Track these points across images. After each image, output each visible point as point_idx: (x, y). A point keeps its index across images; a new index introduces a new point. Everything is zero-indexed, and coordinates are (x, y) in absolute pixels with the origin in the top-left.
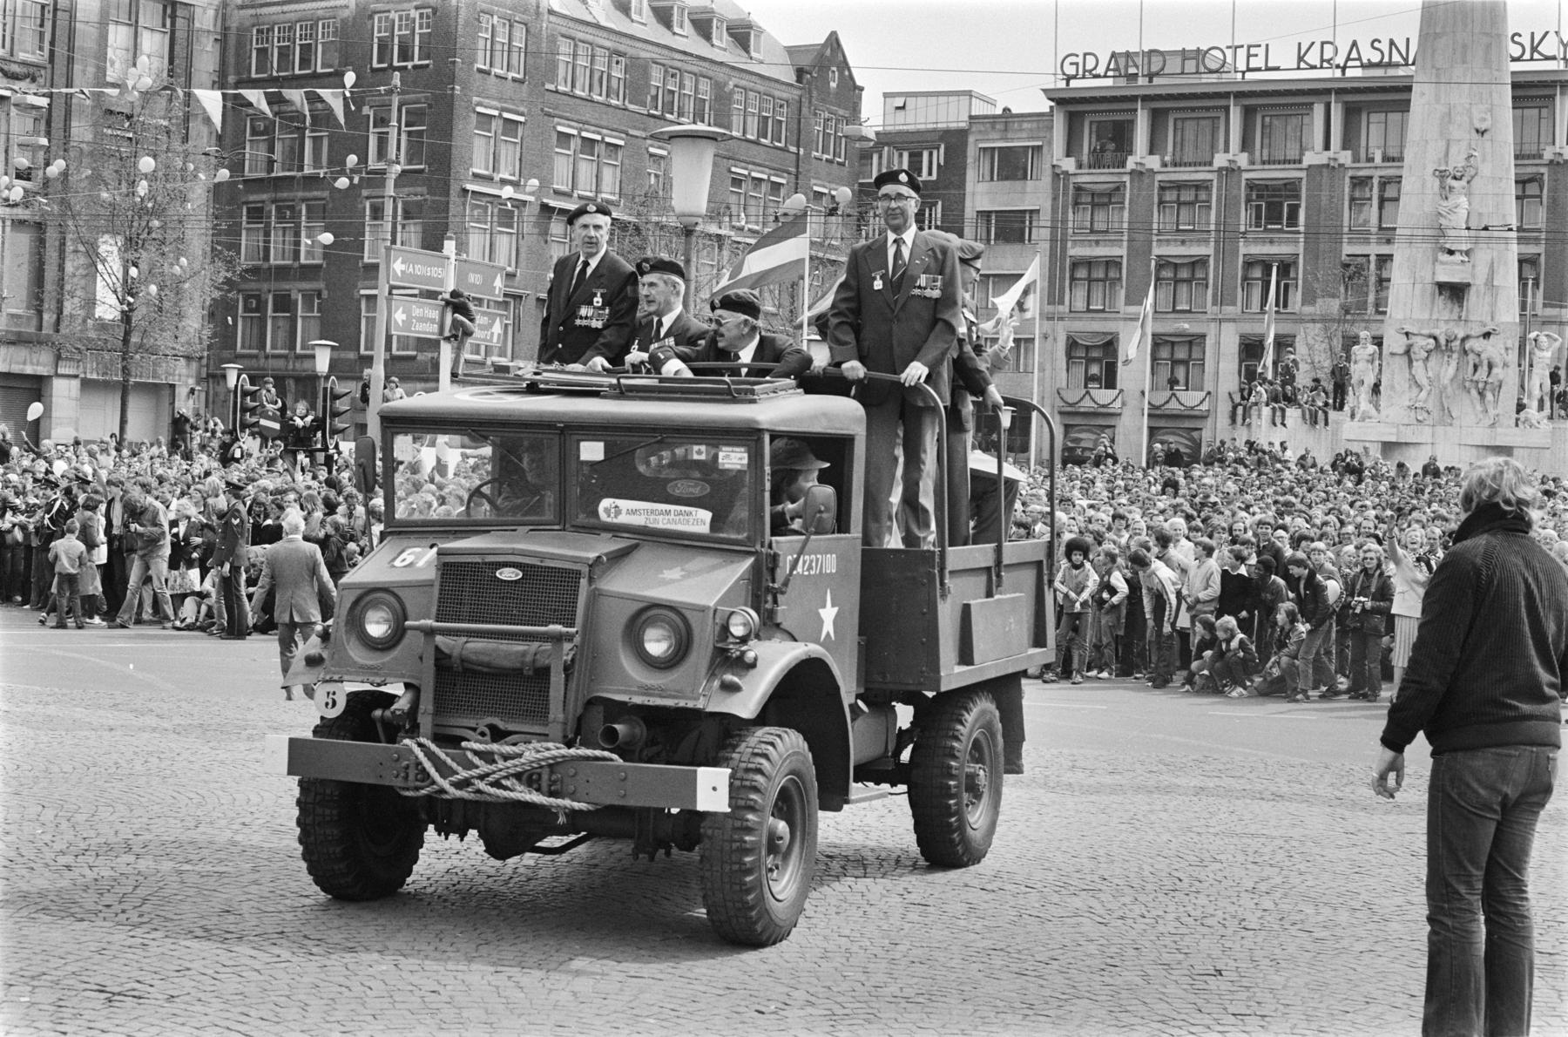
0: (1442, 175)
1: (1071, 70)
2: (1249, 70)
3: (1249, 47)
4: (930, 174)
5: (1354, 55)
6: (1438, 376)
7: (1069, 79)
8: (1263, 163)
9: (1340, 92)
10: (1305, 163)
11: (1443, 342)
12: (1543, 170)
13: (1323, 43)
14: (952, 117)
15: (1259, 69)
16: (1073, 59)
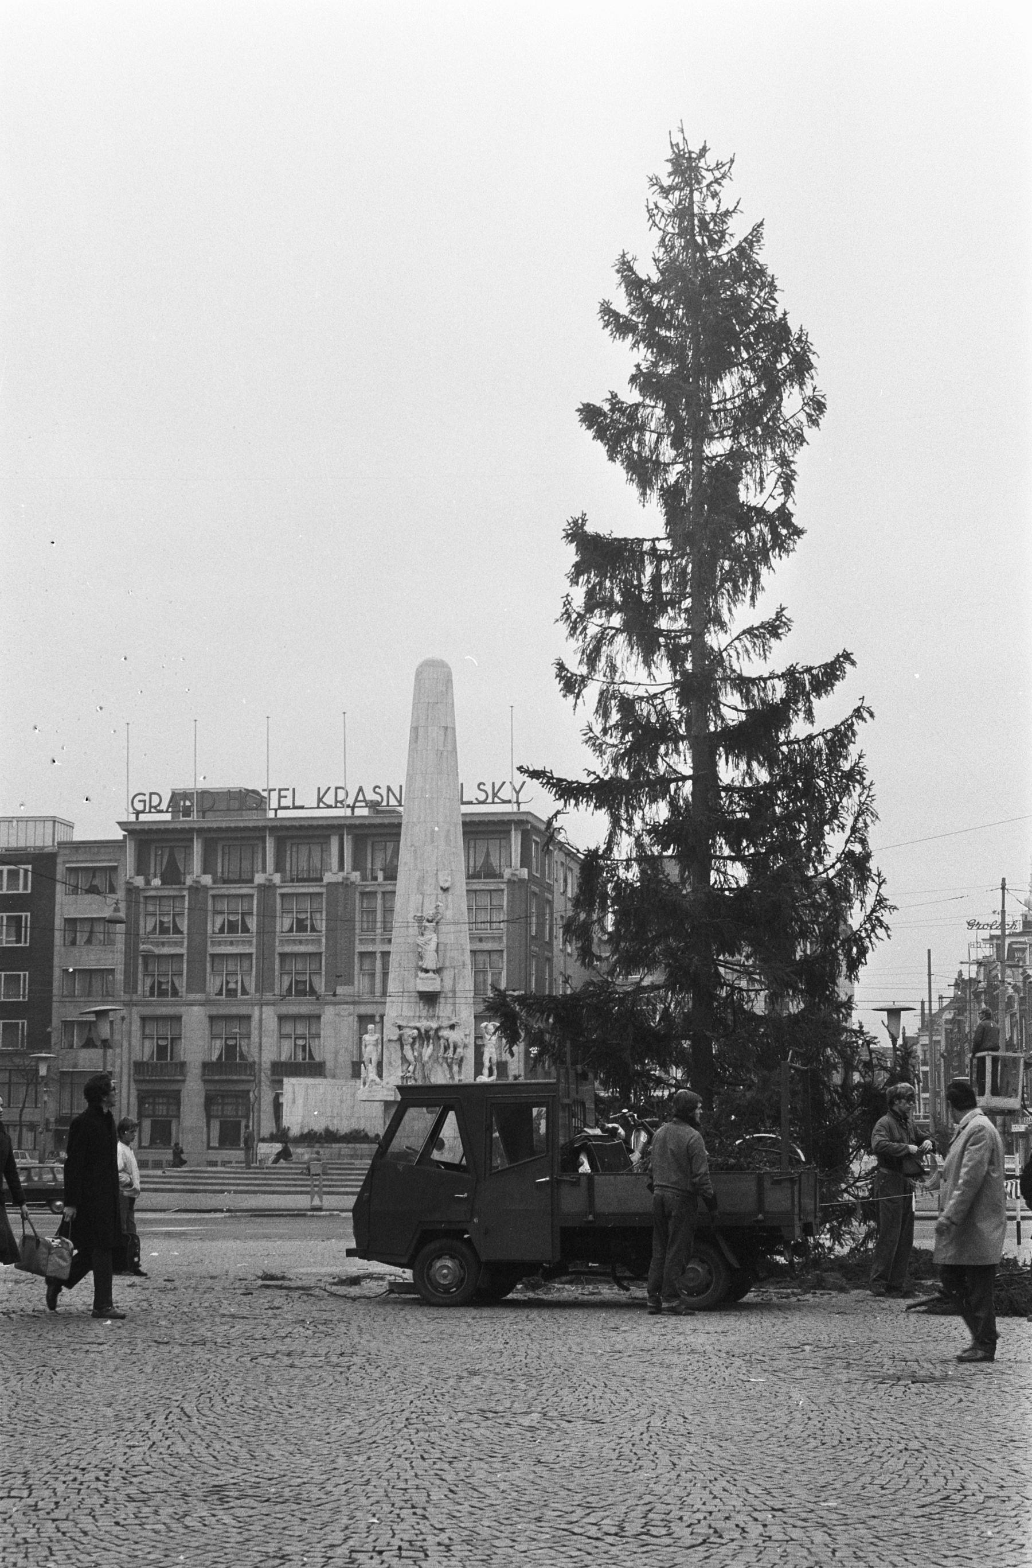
0: (420, 920)
1: (139, 806)
3: (280, 790)
4: (25, 887)
5: (361, 798)
6: (420, 1054)
7: (138, 813)
8: (292, 881)
9: (351, 827)
10: (326, 880)
11: (423, 1031)
12: (503, 886)
13: (337, 788)
14: (40, 839)
15: (288, 808)
16: (141, 797)
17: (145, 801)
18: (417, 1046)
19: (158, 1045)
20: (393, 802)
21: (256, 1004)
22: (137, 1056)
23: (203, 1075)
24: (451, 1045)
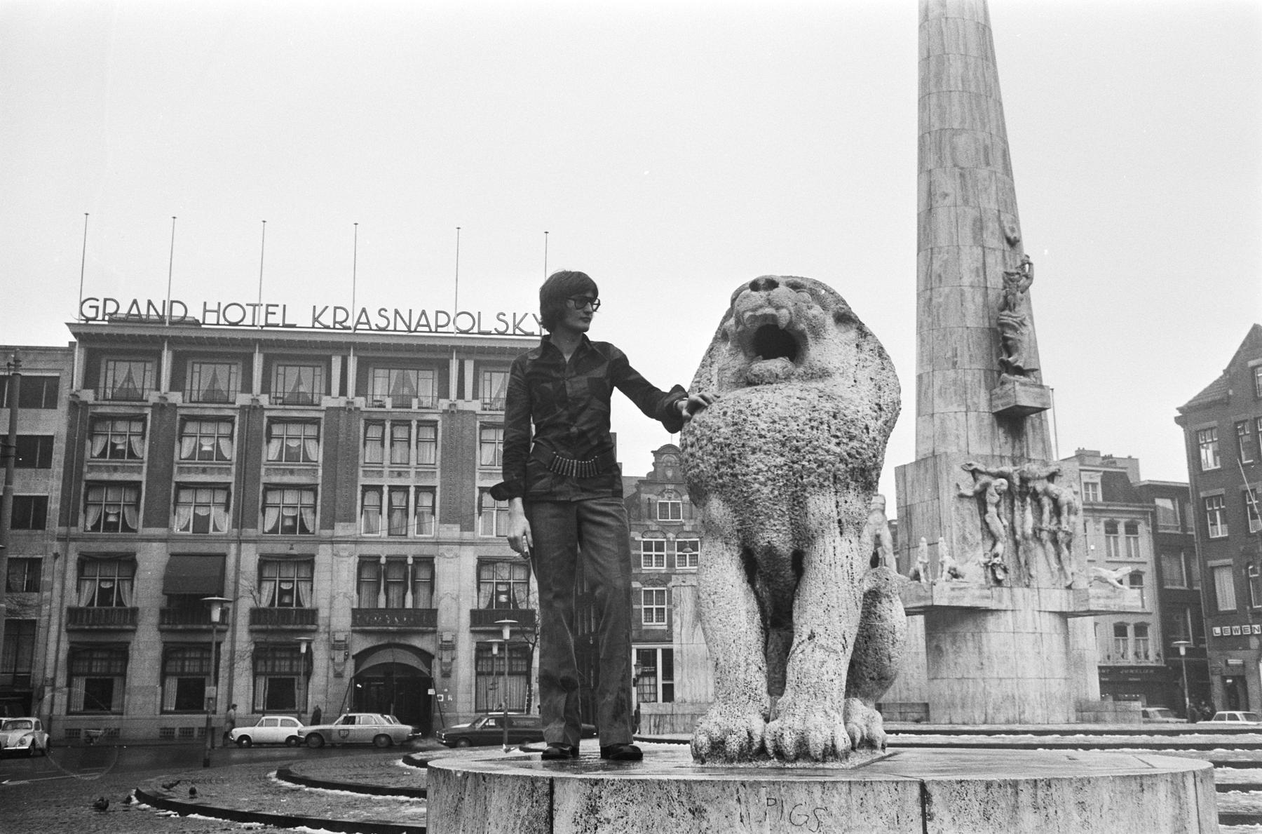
2: (267, 325)
3: (268, 306)
5: (363, 319)
6: (1012, 523)
7: (88, 319)
9: (359, 347)
13: (336, 308)
15: (277, 326)
17: (97, 308)
18: (1002, 509)
19: (100, 587)
20: (401, 326)
21: (233, 541)
22: (72, 600)
23: (162, 623)
24: (1065, 508)
